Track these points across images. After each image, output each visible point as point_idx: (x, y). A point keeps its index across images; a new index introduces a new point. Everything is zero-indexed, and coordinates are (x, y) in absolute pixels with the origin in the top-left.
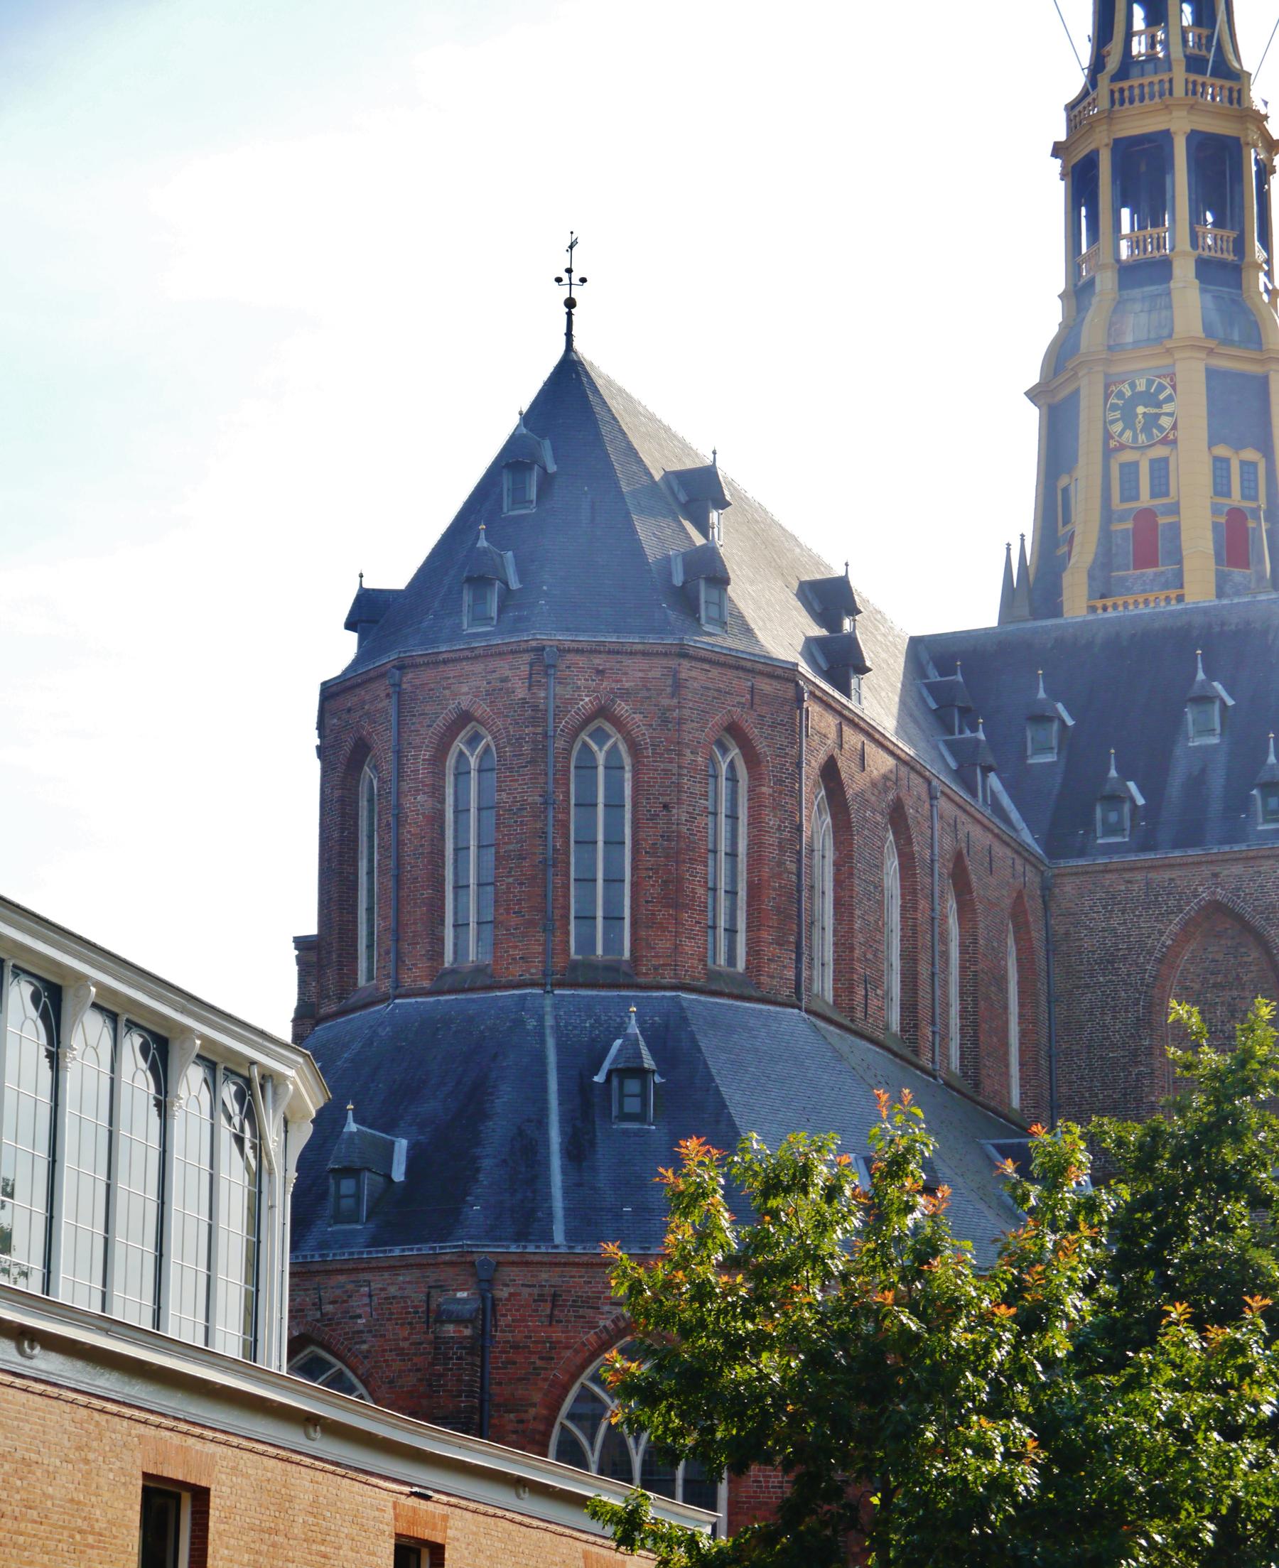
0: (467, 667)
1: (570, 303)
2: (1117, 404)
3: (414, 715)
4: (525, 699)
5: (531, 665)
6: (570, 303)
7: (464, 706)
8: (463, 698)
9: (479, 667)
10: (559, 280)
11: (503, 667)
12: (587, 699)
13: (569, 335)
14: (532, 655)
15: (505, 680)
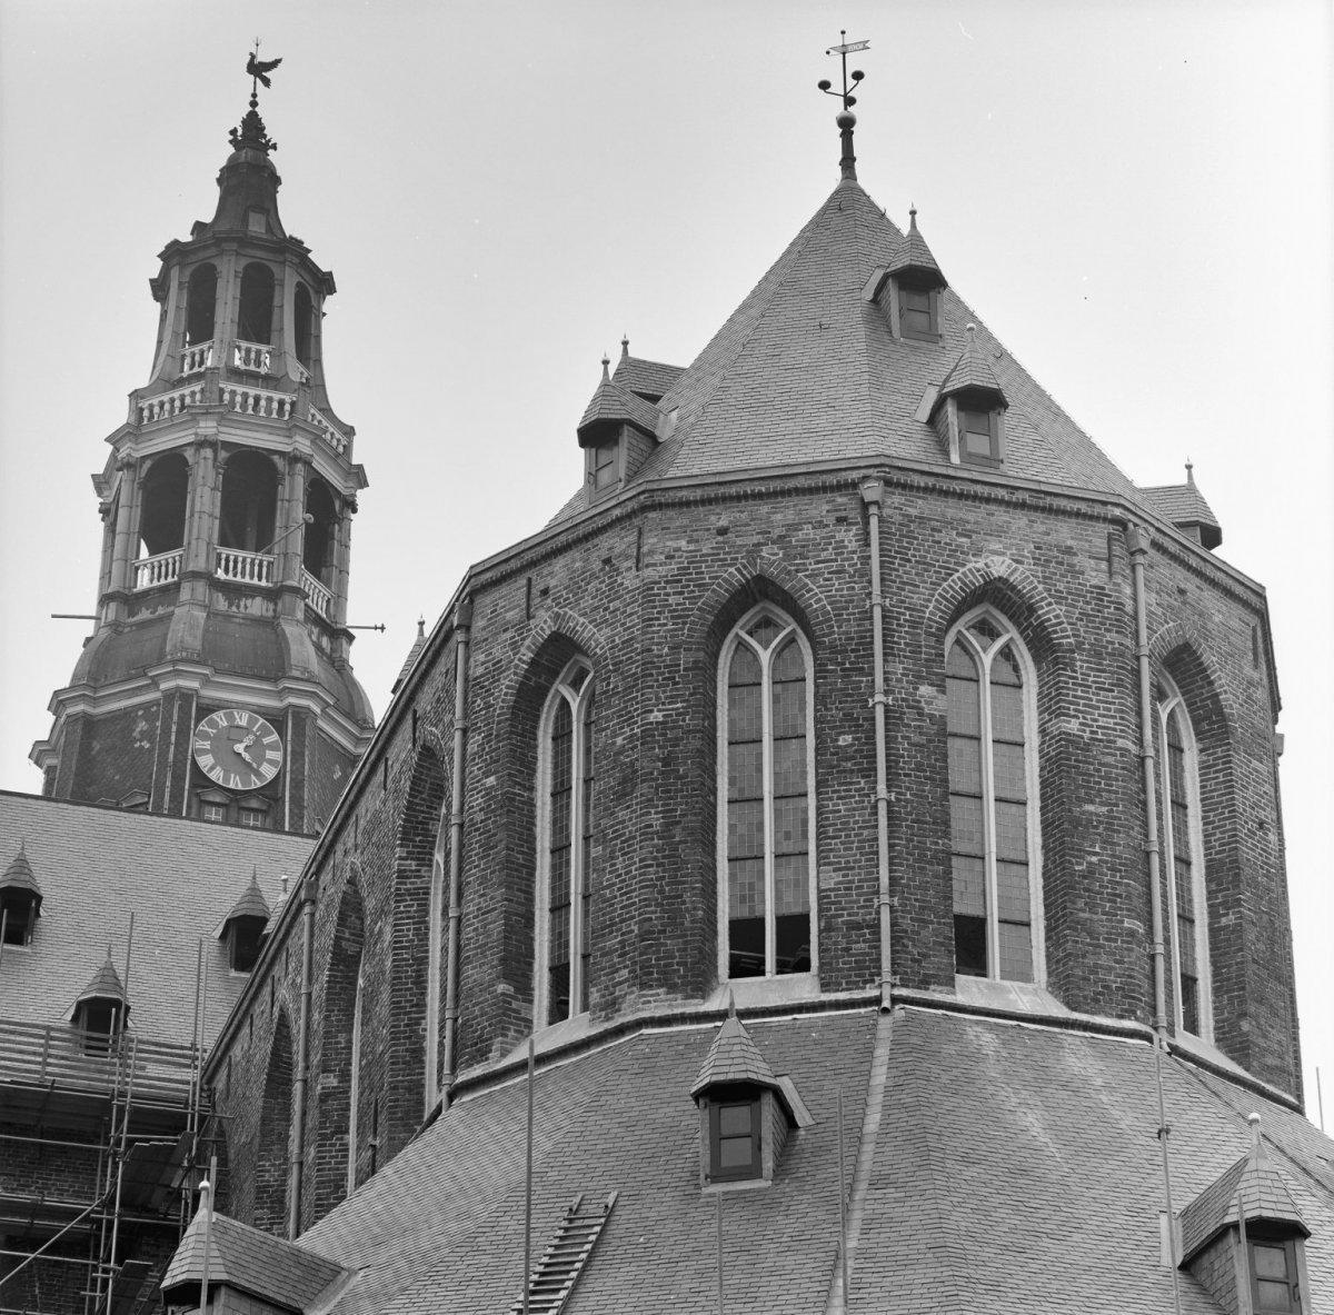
0: (1001, 516)
1: (846, 125)
2: (207, 732)
3: (909, 561)
4: (1103, 589)
5: (1110, 538)
6: (846, 125)
7: (1000, 567)
8: (995, 558)
9: (1020, 520)
10: (824, 85)
11: (1064, 532)
12: (1171, 624)
13: (848, 161)
14: (1111, 528)
15: (1069, 551)
